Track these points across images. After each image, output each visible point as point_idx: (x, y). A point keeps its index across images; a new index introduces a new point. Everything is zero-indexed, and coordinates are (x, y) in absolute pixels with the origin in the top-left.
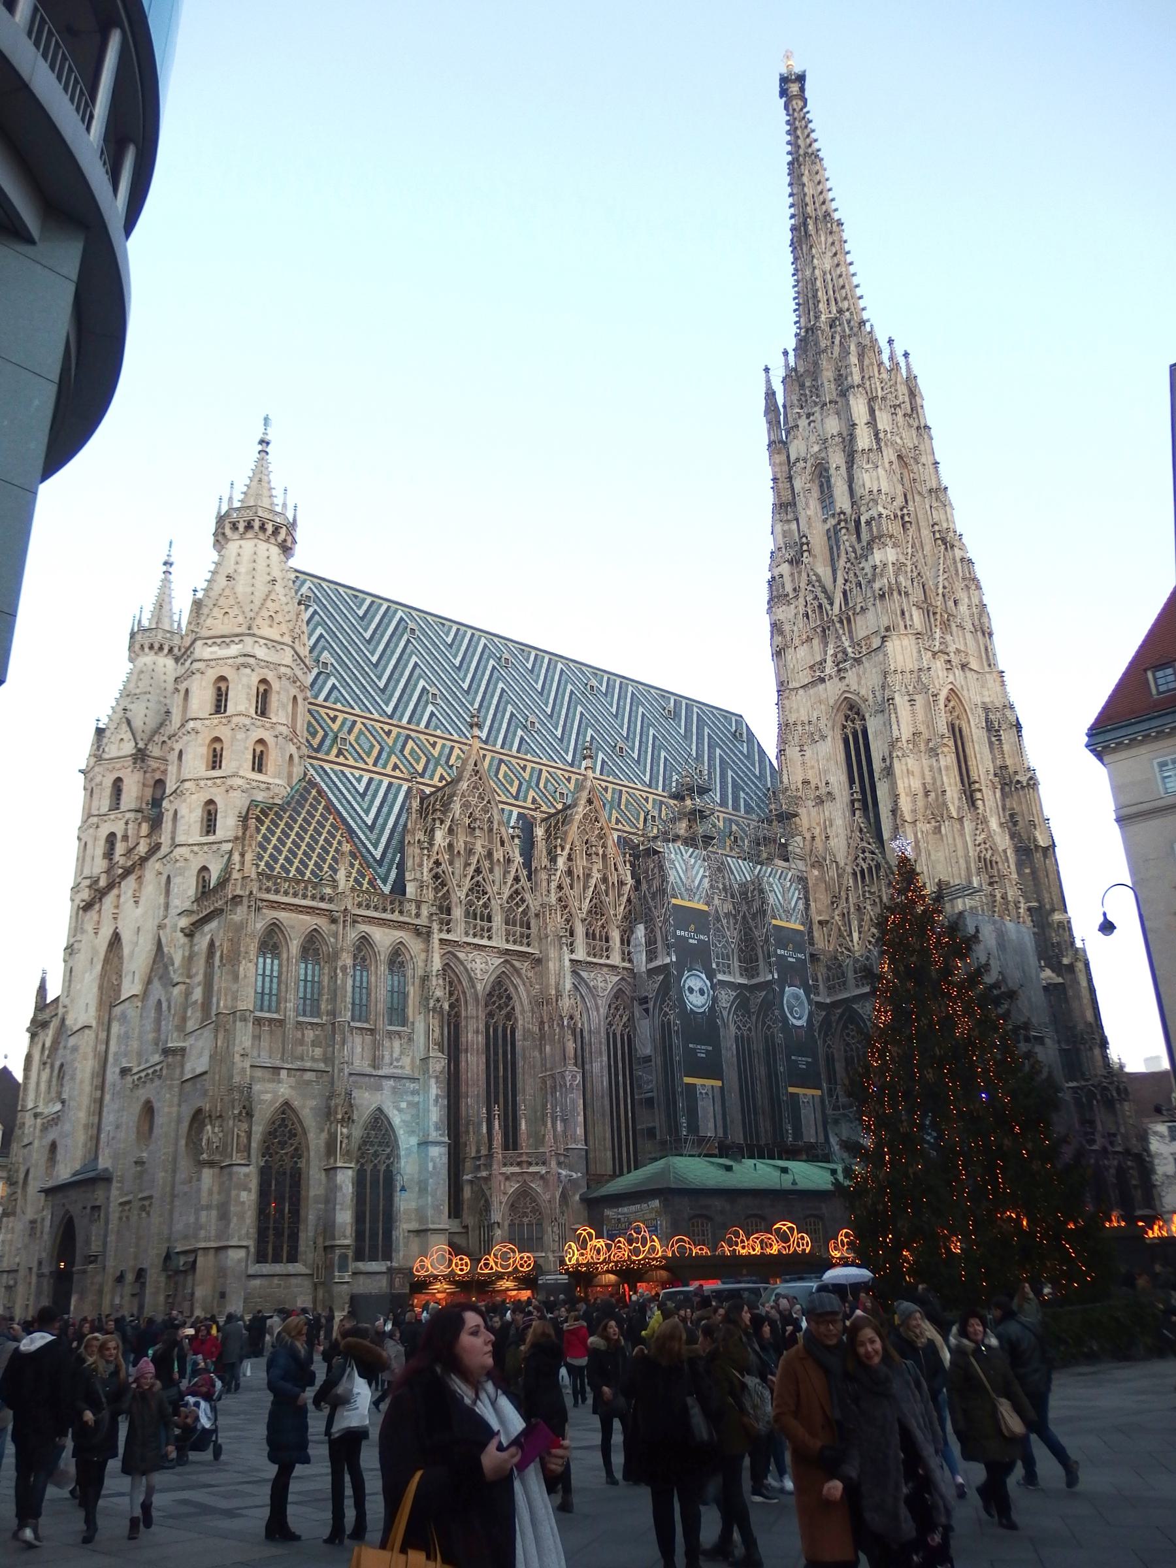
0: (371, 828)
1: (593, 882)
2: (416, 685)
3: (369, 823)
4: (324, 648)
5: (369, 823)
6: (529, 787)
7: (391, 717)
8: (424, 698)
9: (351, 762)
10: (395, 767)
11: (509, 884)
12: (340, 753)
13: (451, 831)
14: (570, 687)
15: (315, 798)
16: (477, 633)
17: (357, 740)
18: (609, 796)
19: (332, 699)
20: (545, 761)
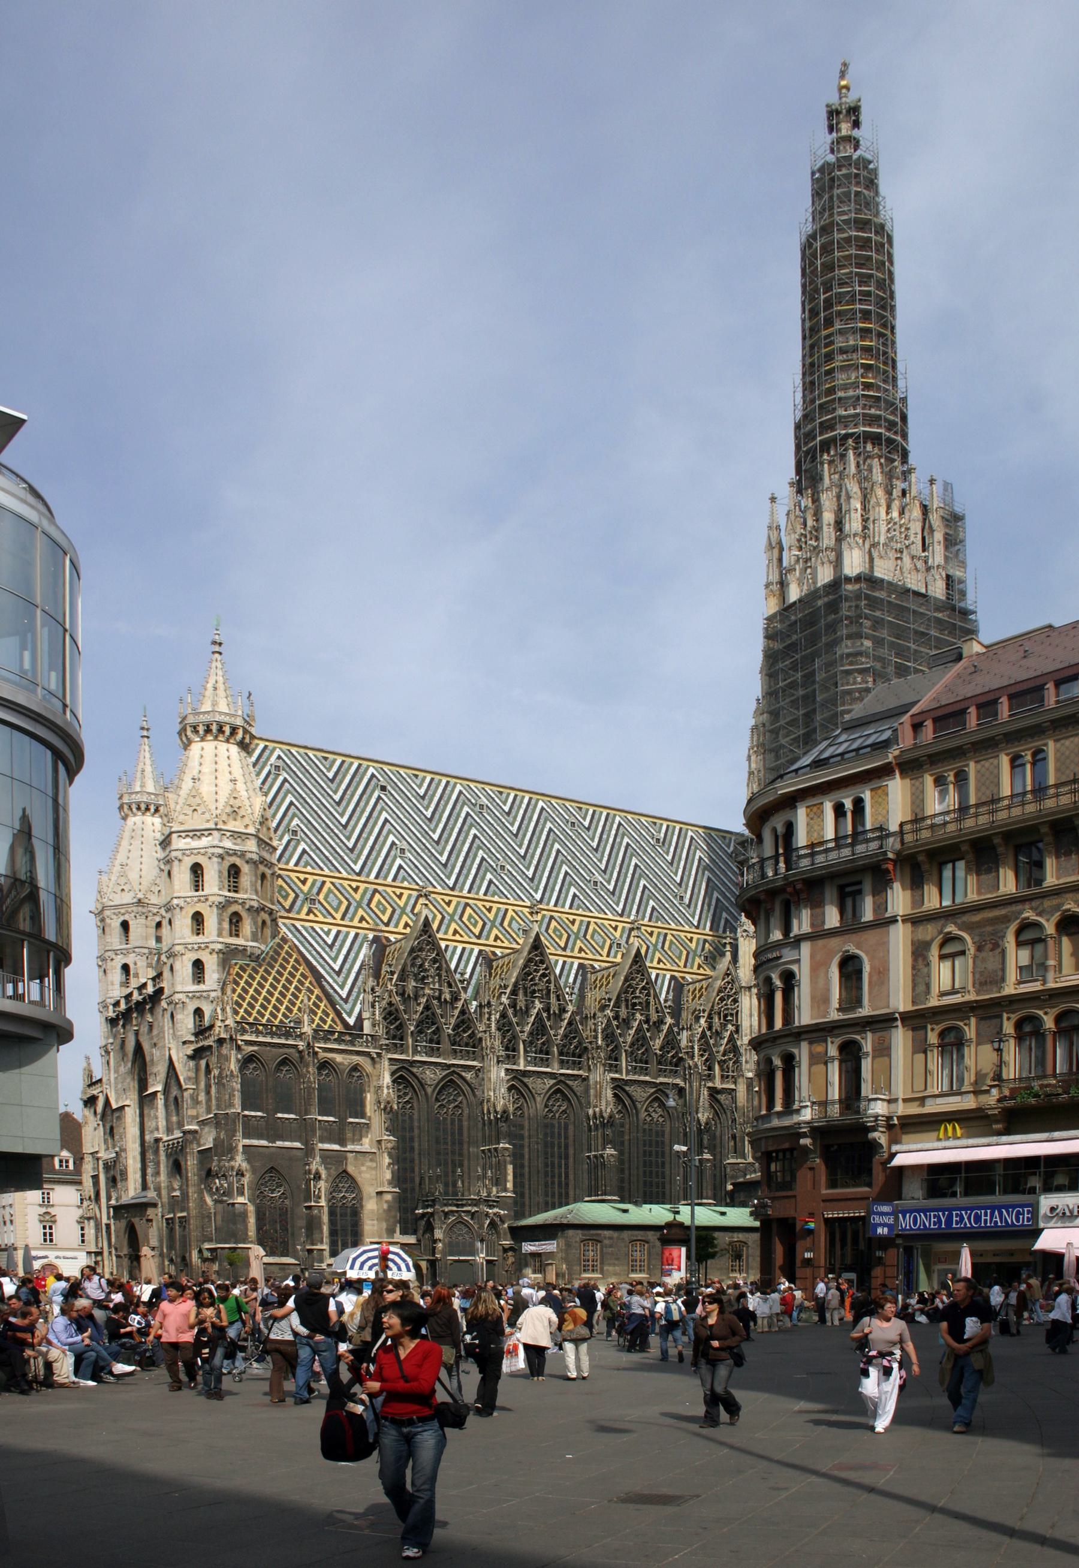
3: (337, 968)
6: (493, 926)
7: (359, 874)
8: (393, 853)
9: (321, 918)
10: (362, 919)
12: (310, 911)
15: (287, 953)
17: (326, 899)
18: (575, 928)
20: (512, 901)
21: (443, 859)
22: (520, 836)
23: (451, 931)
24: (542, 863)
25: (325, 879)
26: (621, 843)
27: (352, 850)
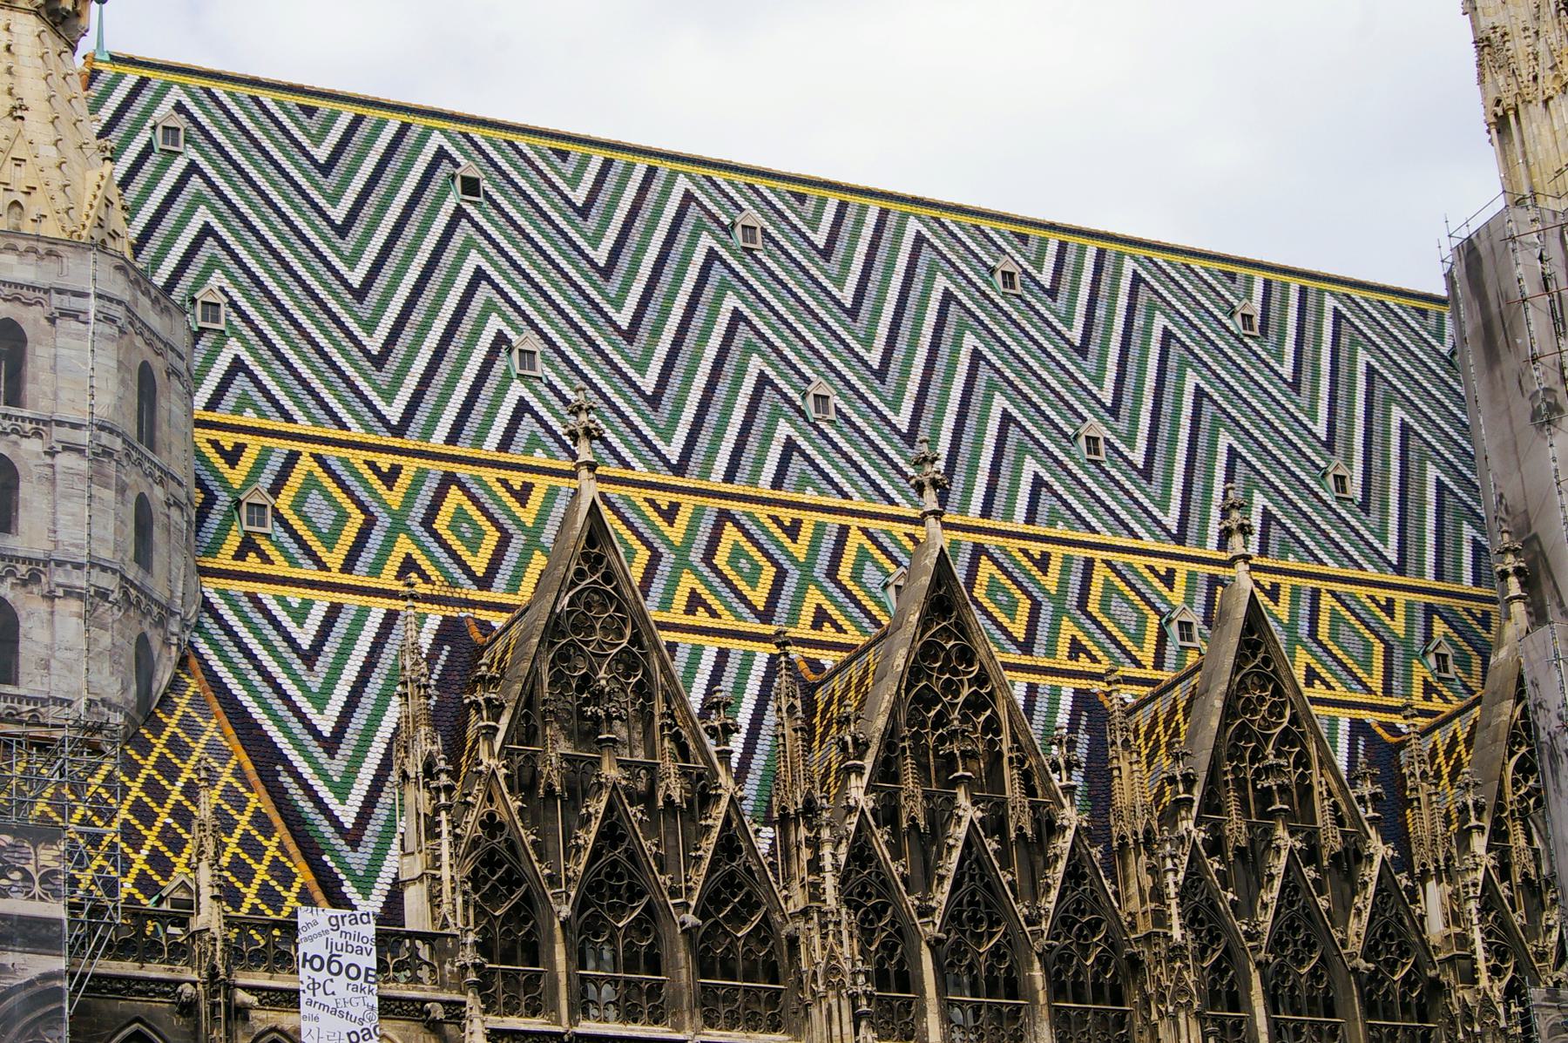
0: (331, 745)
1: (961, 832)
2: (476, 334)
3: (326, 728)
4: (213, 264)
5: (326, 728)
6: (807, 579)
7: (399, 430)
8: (499, 368)
9: (281, 568)
11: (705, 864)
12: (248, 546)
13: (525, 730)
14: (941, 283)
16: (665, 167)
17: (297, 507)
18: (1051, 581)
19: (230, 399)
20: (857, 503)
21: (648, 383)
22: (864, 313)
23: (681, 599)
24: (933, 391)
25: (296, 446)
26: (1147, 332)
27: (379, 361)
